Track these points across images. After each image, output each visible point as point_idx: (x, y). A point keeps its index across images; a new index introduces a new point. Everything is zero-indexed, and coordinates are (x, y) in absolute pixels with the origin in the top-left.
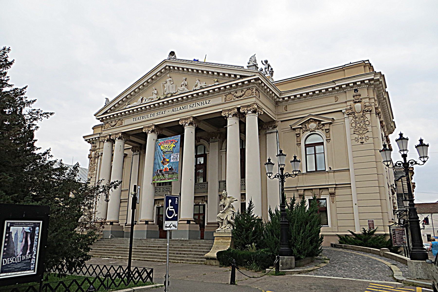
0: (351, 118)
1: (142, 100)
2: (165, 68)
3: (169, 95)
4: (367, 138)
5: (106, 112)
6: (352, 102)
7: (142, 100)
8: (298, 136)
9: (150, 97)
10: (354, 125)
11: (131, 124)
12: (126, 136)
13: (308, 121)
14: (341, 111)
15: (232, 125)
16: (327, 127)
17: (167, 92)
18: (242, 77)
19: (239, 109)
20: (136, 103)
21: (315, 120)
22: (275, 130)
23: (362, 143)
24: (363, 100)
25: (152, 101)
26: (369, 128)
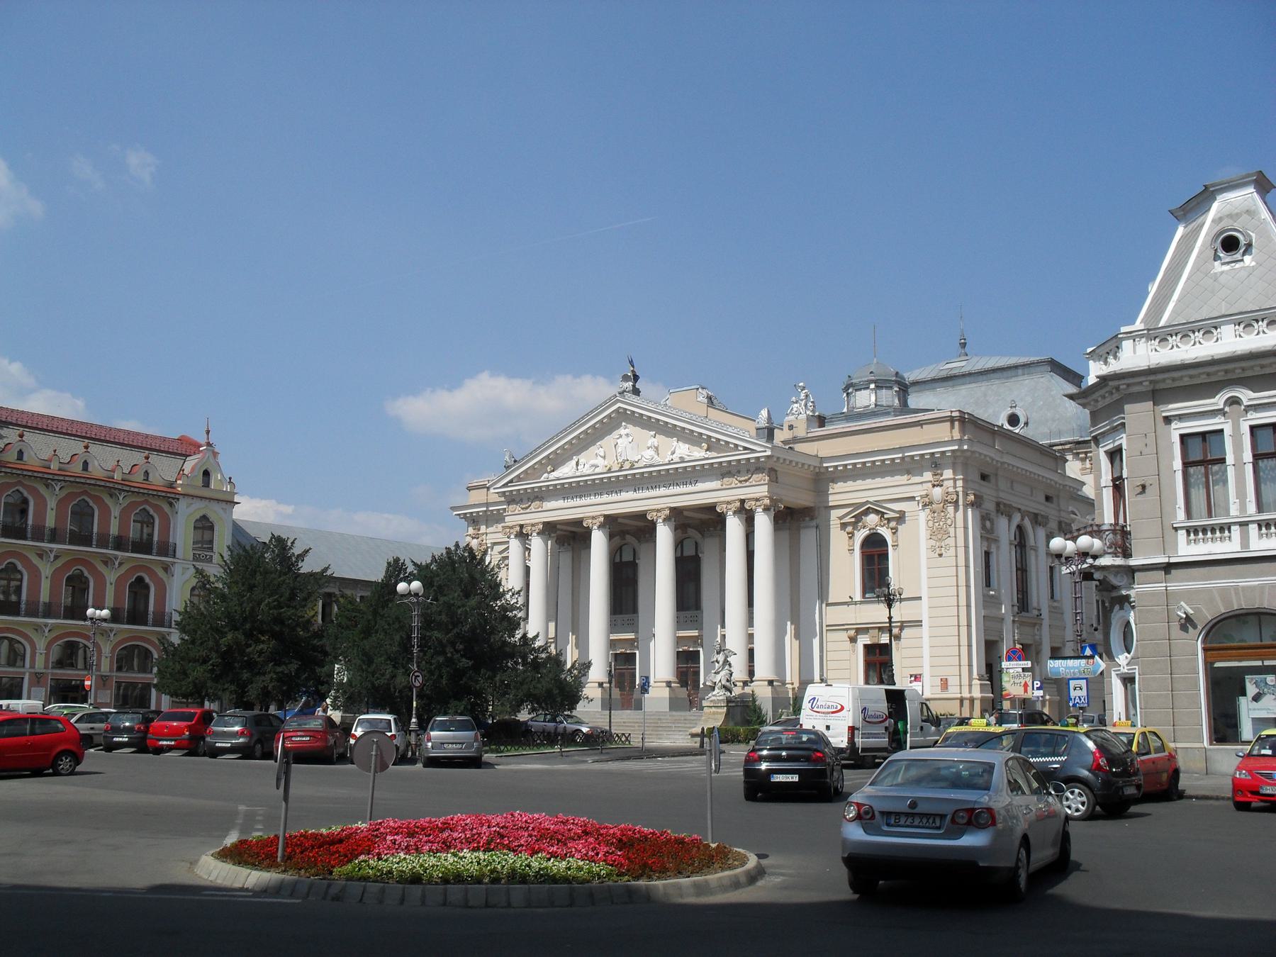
0: (928, 511)
1: (577, 464)
2: (617, 411)
3: (627, 466)
4: (947, 547)
5: (511, 481)
6: (930, 485)
7: (577, 464)
8: (851, 536)
9: (592, 463)
10: (931, 524)
11: (560, 510)
12: (549, 529)
13: (867, 512)
14: (913, 498)
15: (734, 527)
16: (893, 524)
17: (624, 457)
18: (745, 448)
19: (743, 501)
20: (566, 471)
21: (877, 512)
22: (814, 523)
23: (940, 555)
24: (945, 483)
25: (597, 470)
26: (952, 530)
